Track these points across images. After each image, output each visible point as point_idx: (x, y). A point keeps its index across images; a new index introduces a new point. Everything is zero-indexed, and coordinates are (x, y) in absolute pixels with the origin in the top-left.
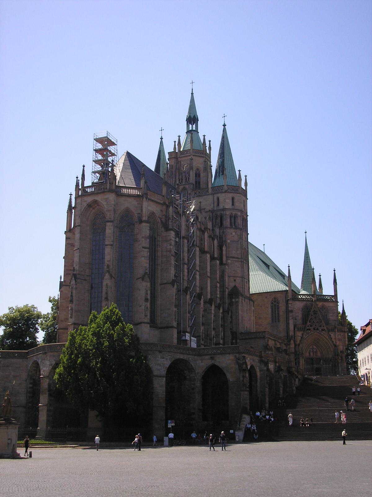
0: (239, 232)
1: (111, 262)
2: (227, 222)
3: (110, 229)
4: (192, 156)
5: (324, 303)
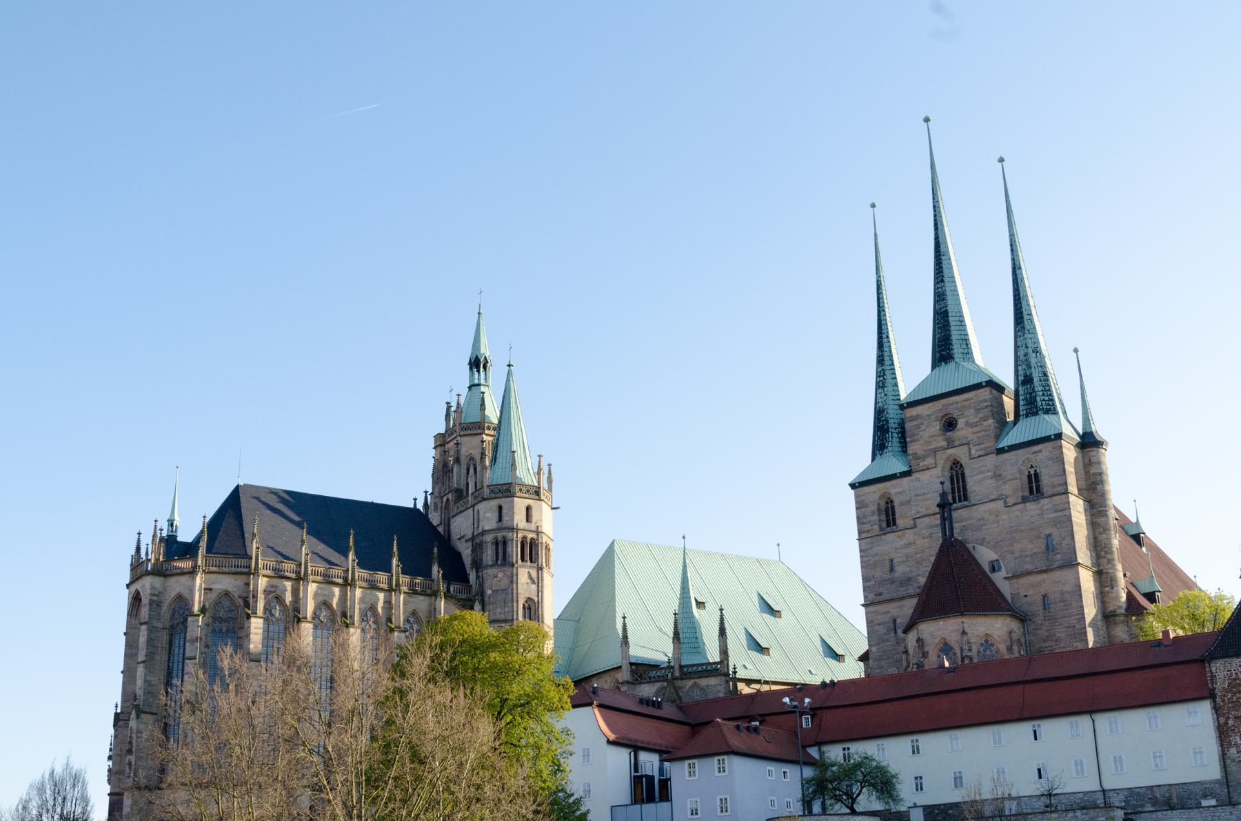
0: (508, 570)
1: (142, 689)
2: (488, 555)
3: (143, 635)
4: (459, 438)
5: (698, 681)
